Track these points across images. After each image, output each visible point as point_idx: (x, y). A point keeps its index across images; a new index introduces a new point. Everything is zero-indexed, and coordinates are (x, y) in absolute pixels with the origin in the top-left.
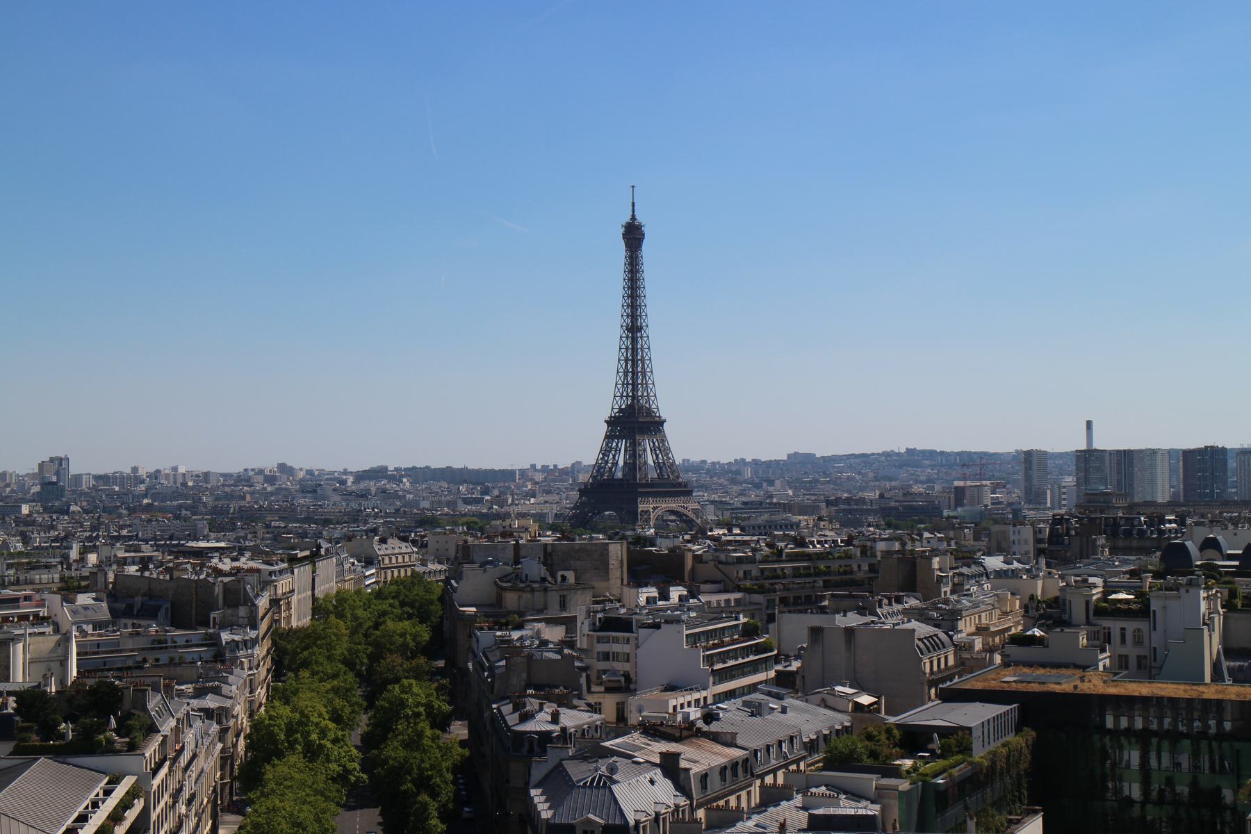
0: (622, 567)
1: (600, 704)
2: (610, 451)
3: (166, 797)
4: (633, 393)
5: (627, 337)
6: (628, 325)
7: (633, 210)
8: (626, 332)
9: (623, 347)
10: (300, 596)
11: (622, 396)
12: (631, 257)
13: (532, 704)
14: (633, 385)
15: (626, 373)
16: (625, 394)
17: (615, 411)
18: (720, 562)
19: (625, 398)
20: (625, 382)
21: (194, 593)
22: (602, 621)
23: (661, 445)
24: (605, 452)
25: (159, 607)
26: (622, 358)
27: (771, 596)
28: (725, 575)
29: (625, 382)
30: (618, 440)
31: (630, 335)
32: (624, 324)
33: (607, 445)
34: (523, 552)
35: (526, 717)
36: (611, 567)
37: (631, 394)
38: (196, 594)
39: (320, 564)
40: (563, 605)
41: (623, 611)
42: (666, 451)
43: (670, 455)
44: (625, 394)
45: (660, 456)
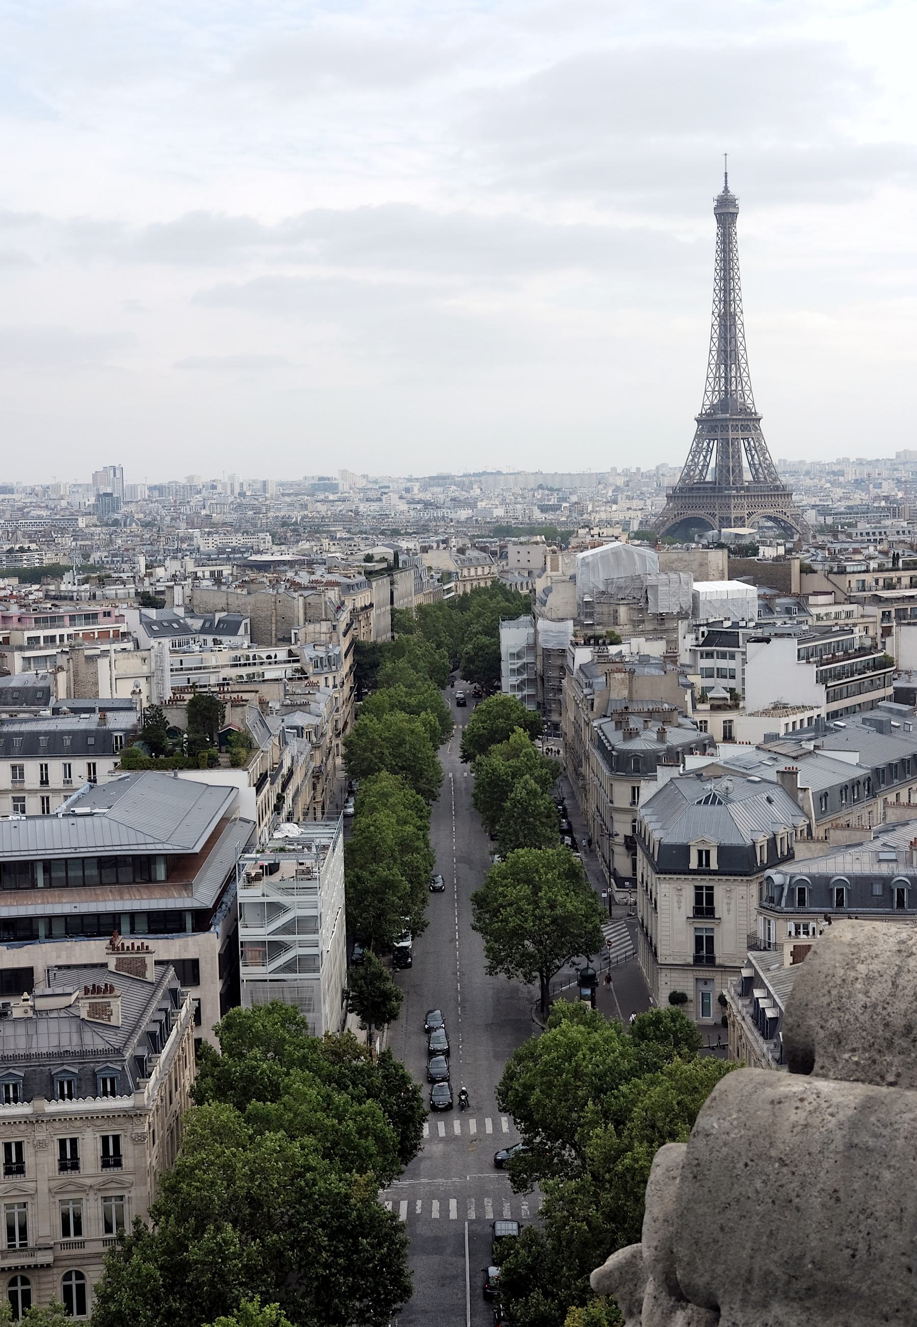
1: (706, 722)
2: (700, 453)
3: (269, 813)
7: (726, 181)
10: (378, 611)
12: (724, 235)
13: (635, 723)
14: (726, 378)
16: (717, 389)
24: (695, 452)
33: (697, 446)
35: (631, 735)
39: (397, 576)
41: (727, 624)
42: (764, 451)
44: (717, 389)
45: (756, 457)
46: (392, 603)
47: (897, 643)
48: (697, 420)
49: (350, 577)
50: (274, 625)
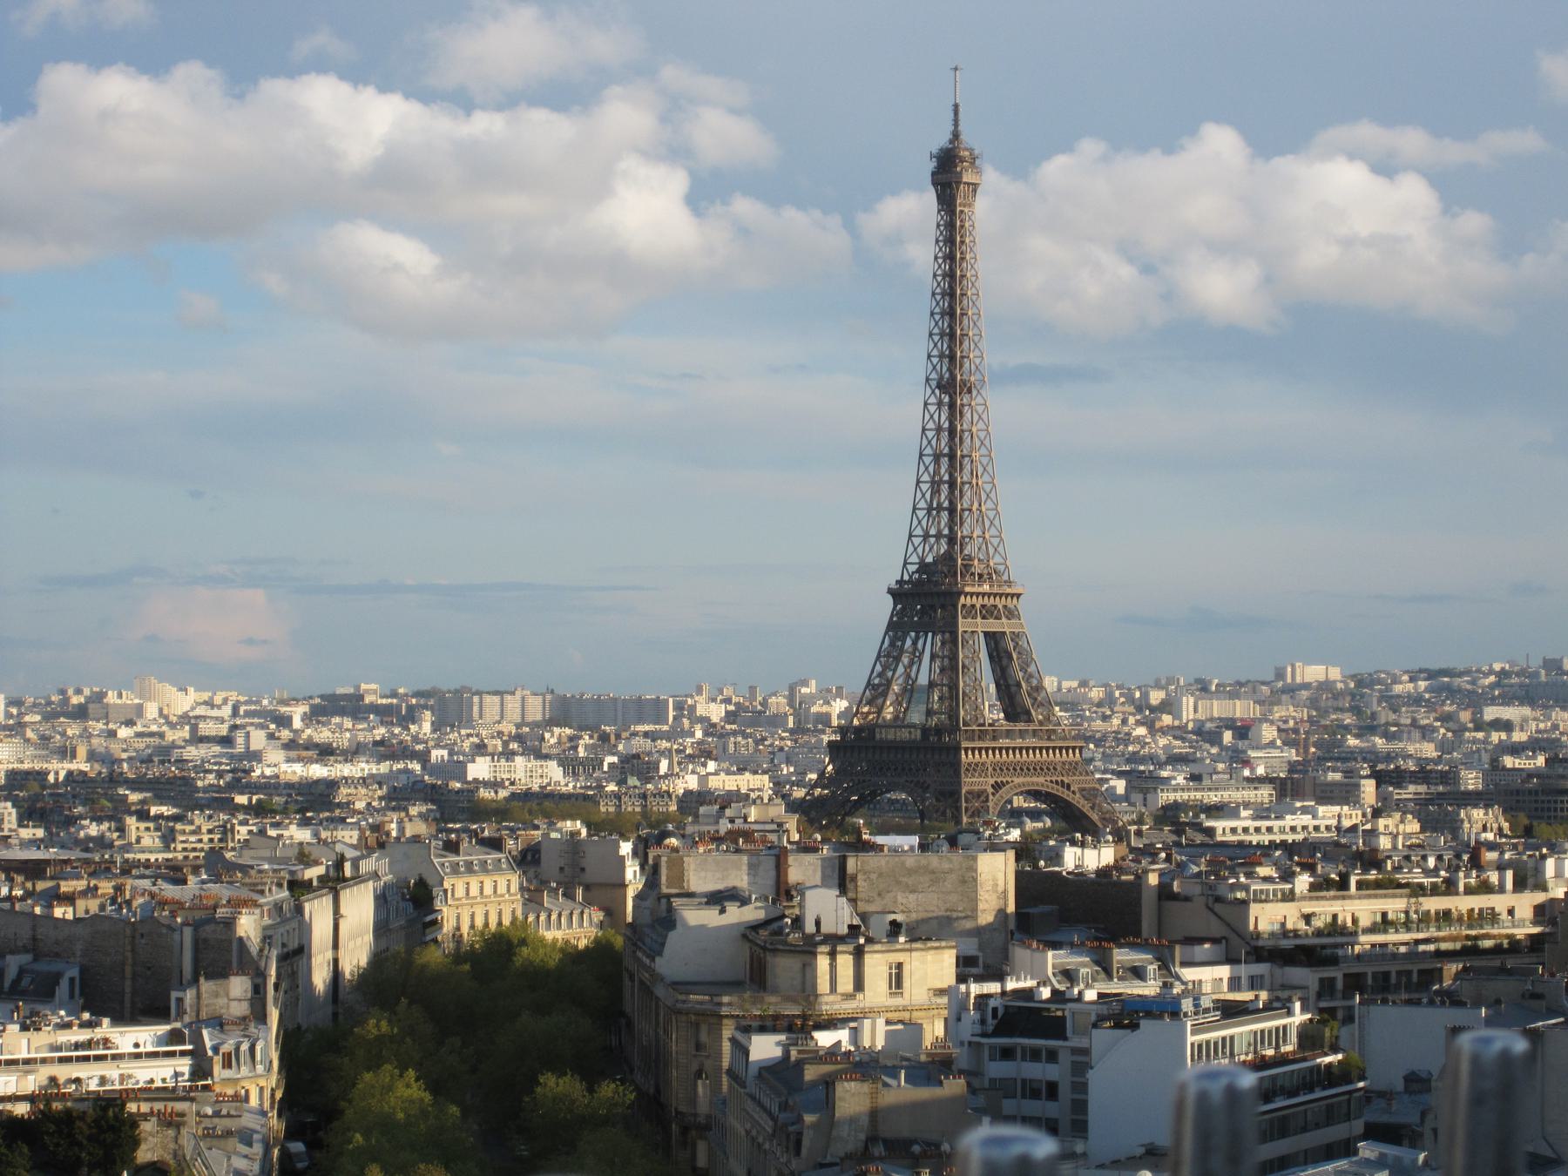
2: (898, 659)
4: (951, 529)
5: (940, 404)
6: (941, 377)
8: (937, 391)
9: (931, 425)
11: (926, 536)
14: (952, 510)
15: (935, 485)
16: (933, 532)
17: (912, 568)
18: (1218, 899)
19: (932, 540)
20: (935, 505)
21: (129, 948)
22: (1000, 1014)
24: (890, 655)
25: (56, 978)
26: (928, 451)
27: (1329, 972)
28: (1228, 925)
29: (935, 505)
30: (917, 633)
31: (947, 399)
32: (934, 376)
33: (892, 644)
34: (794, 875)
37: (946, 532)
38: (133, 951)
39: (346, 896)
40: (897, 980)
43: (1032, 669)
46: (336, 946)
47: (1361, 1037)
48: (897, 594)
49: (262, 892)
50: (128, 983)
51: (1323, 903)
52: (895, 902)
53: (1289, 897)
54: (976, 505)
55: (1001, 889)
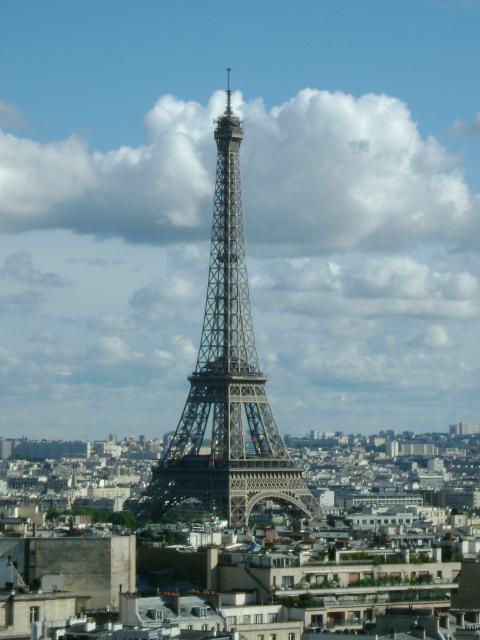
0: (129, 569)
2: (194, 418)
5: (219, 268)
6: (219, 252)
11: (211, 346)
12: (225, 163)
14: (225, 331)
15: (216, 316)
16: (214, 343)
18: (253, 565)
23: (260, 411)
24: (189, 417)
26: (212, 296)
31: (223, 266)
32: (215, 251)
33: (190, 410)
36: (113, 570)
40: (35, 615)
43: (272, 425)
45: (259, 425)
51: (317, 568)
52: (59, 567)
53: (297, 564)
54: (240, 328)
55: (126, 558)
